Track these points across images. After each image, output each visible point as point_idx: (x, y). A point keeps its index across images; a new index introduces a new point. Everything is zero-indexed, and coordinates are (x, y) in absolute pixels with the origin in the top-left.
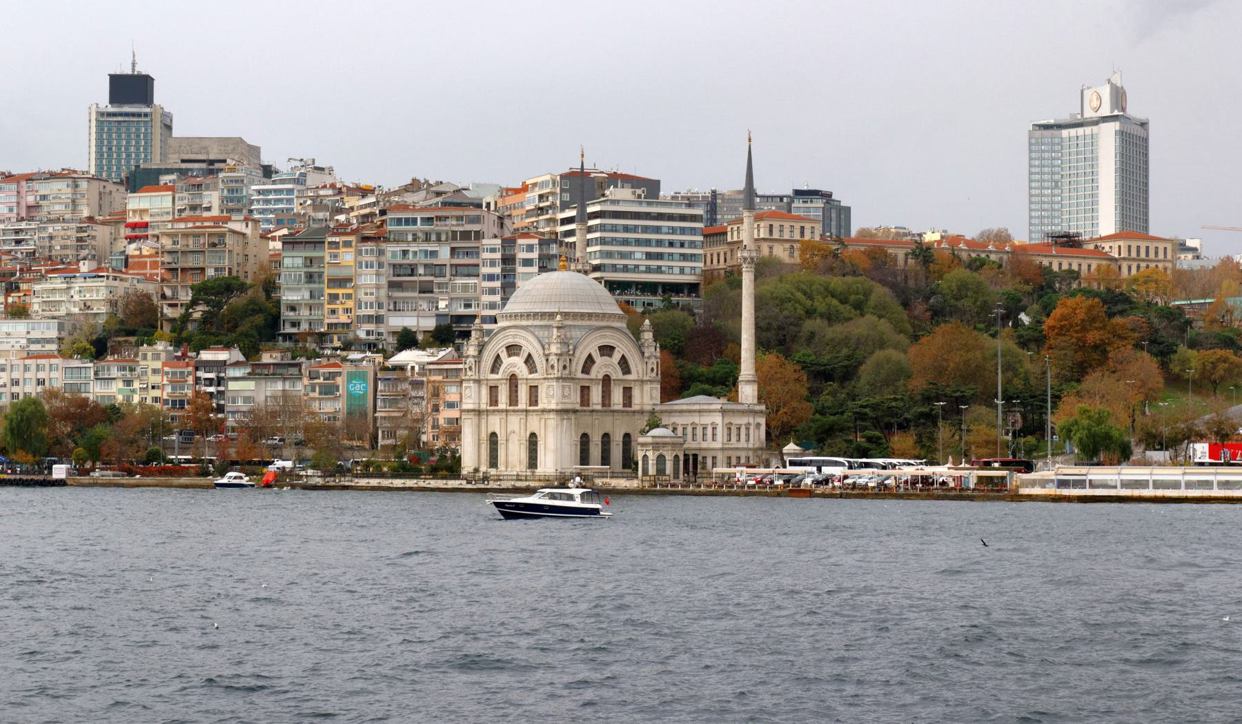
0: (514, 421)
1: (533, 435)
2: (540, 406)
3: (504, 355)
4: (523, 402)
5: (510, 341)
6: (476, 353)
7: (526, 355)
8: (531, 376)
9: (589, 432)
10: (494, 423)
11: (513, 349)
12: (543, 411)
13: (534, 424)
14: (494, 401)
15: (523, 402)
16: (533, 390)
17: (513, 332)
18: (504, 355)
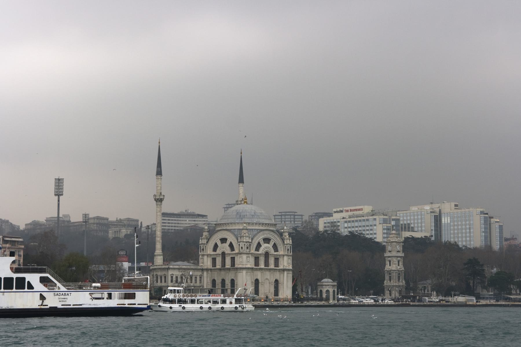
0: (267, 275)
1: (277, 281)
2: (281, 267)
3: (262, 242)
4: (272, 266)
5: (265, 236)
6: (250, 241)
7: (273, 243)
8: (276, 253)
9: (278, 279)
10: (259, 275)
11: (267, 240)
12: (284, 270)
13: (277, 276)
14: (257, 263)
15: (272, 266)
16: (277, 260)
17: (267, 232)
18: (262, 242)
